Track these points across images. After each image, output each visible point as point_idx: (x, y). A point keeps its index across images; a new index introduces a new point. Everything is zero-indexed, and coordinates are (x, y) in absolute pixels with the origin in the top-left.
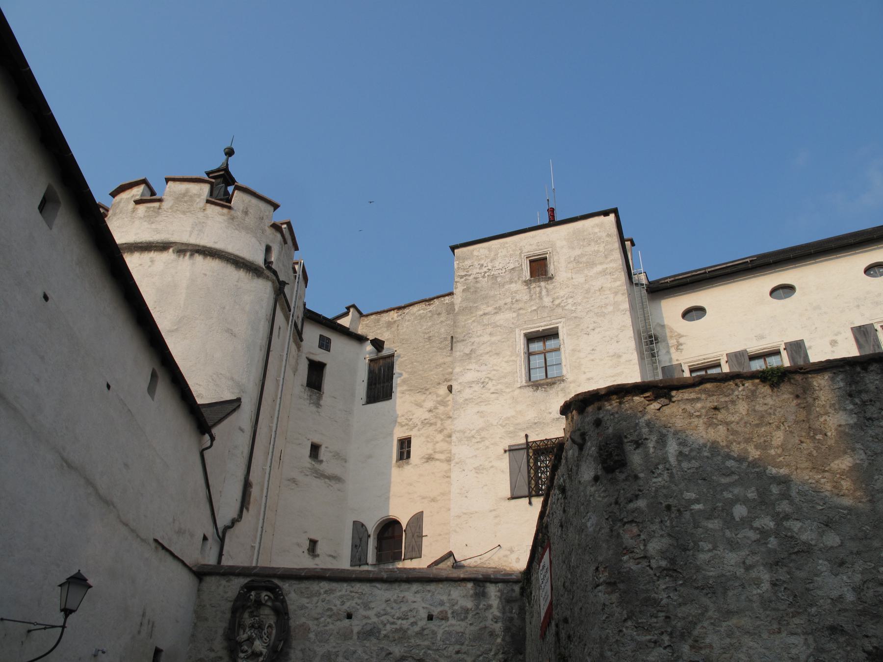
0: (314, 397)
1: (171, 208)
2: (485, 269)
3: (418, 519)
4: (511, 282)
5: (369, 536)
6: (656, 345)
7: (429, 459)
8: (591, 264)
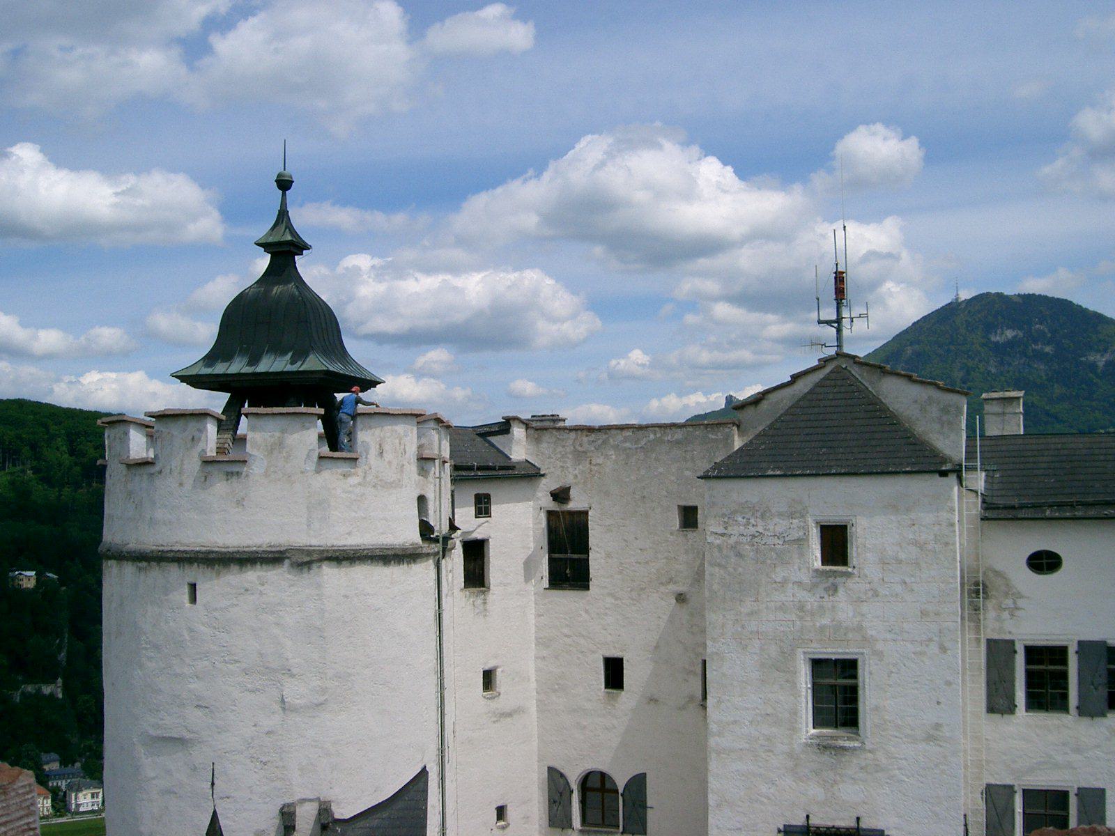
0: (479, 601)
1: (266, 475)
2: (752, 530)
3: (638, 782)
5: (572, 792)
6: (983, 601)
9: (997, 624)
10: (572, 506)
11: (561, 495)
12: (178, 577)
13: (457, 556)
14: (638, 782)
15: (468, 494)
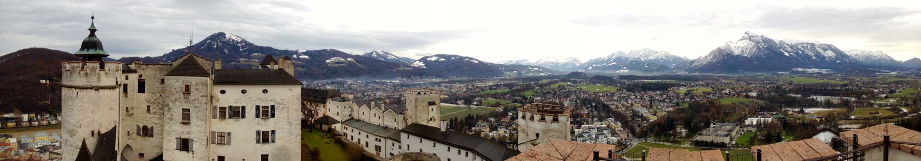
3: (152, 128)
7: (155, 113)
10: (142, 78)
11: (140, 76)
13: (122, 87)
14: (152, 128)
15: (124, 76)
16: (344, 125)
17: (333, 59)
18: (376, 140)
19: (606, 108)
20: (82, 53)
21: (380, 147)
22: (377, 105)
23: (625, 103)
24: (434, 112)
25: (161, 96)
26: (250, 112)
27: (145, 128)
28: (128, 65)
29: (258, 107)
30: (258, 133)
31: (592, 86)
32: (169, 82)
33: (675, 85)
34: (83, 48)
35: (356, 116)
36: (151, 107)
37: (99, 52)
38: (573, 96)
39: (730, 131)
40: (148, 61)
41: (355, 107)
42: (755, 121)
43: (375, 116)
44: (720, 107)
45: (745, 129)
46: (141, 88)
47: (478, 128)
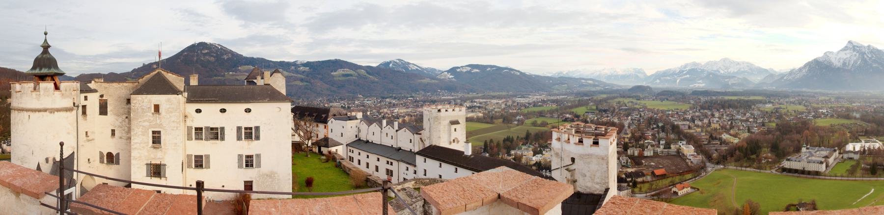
4: (148, 112)
8: (171, 112)
9: (189, 123)
10: (104, 98)
12: (26, 114)
13: (80, 109)
15: (83, 95)
16: (349, 148)
17: (340, 72)
18: (388, 163)
19: (675, 129)
20: (34, 72)
21: (392, 171)
22: (390, 123)
23: (700, 123)
24: (460, 132)
25: (127, 117)
26: (230, 134)
27: (110, 155)
28: (85, 81)
29: (239, 129)
30: (240, 156)
31: (659, 102)
32: (135, 101)
33: (760, 102)
34: (34, 68)
35: (363, 138)
36: (116, 131)
37: (53, 71)
38: (635, 115)
39: (827, 157)
40: (111, 78)
41: (364, 126)
42: (858, 147)
43: (387, 136)
44: (817, 129)
45: (845, 156)
46: (103, 110)
47: (519, 153)
